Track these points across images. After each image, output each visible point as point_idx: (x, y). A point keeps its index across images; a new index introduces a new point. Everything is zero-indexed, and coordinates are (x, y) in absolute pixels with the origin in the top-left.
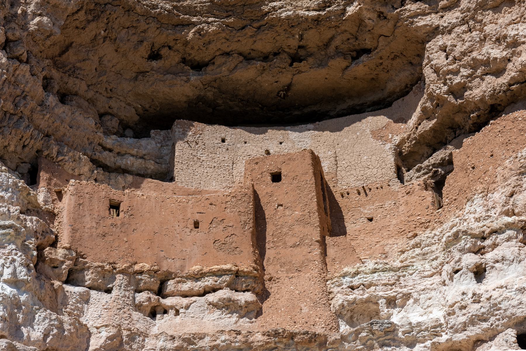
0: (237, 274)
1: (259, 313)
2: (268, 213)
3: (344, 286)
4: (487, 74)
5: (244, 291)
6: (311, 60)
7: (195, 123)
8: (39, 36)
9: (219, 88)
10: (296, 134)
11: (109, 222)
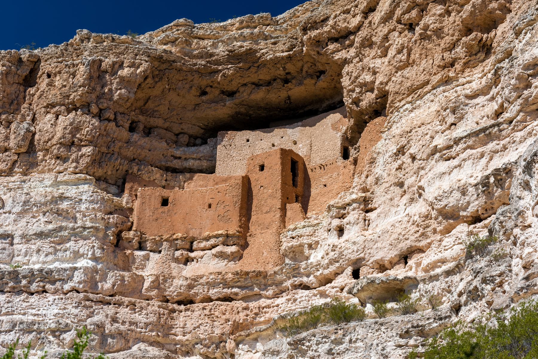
0: (227, 236)
1: (241, 258)
2: (255, 191)
3: (288, 237)
4: (367, 91)
5: (232, 245)
7: (229, 132)
8: (121, 102)
9: (247, 105)
10: (291, 130)
11: (160, 211)
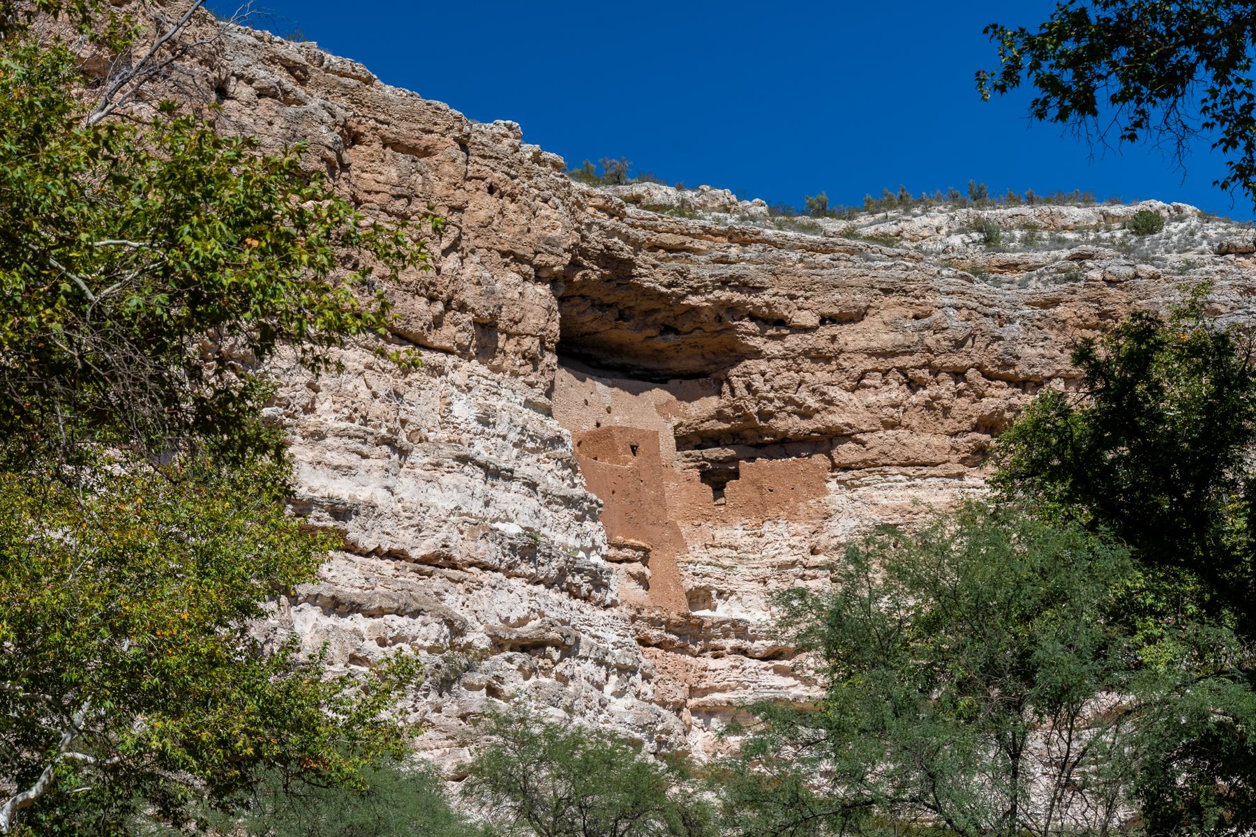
6: (632, 322)
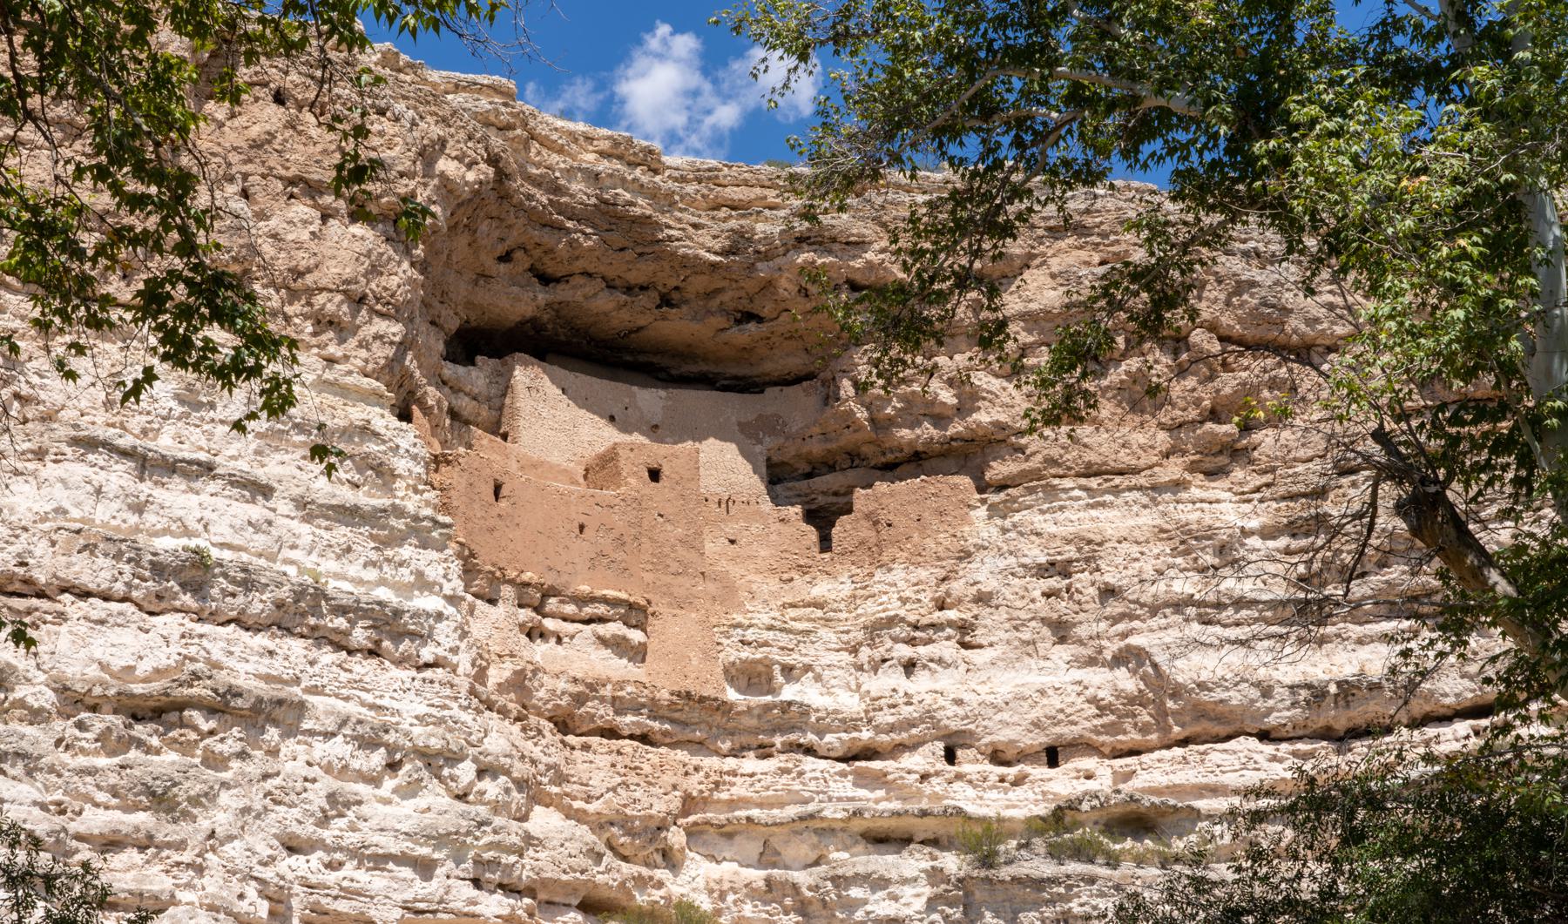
6: (685, 308)
